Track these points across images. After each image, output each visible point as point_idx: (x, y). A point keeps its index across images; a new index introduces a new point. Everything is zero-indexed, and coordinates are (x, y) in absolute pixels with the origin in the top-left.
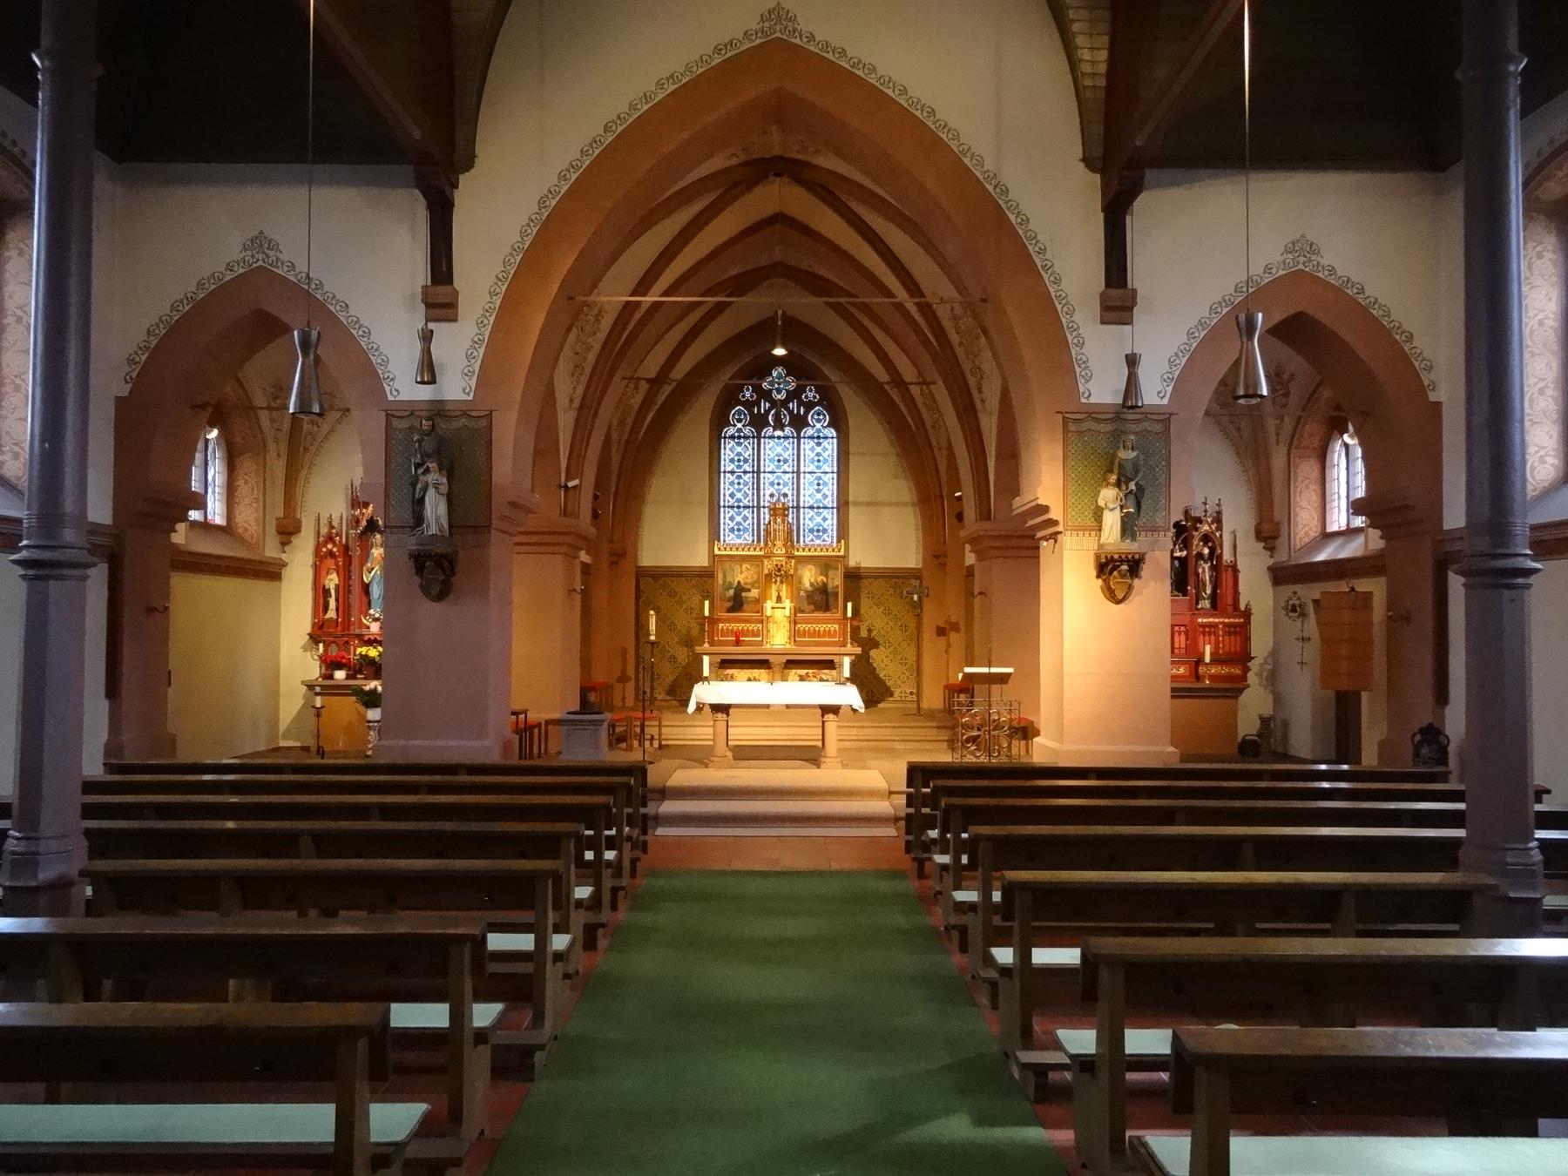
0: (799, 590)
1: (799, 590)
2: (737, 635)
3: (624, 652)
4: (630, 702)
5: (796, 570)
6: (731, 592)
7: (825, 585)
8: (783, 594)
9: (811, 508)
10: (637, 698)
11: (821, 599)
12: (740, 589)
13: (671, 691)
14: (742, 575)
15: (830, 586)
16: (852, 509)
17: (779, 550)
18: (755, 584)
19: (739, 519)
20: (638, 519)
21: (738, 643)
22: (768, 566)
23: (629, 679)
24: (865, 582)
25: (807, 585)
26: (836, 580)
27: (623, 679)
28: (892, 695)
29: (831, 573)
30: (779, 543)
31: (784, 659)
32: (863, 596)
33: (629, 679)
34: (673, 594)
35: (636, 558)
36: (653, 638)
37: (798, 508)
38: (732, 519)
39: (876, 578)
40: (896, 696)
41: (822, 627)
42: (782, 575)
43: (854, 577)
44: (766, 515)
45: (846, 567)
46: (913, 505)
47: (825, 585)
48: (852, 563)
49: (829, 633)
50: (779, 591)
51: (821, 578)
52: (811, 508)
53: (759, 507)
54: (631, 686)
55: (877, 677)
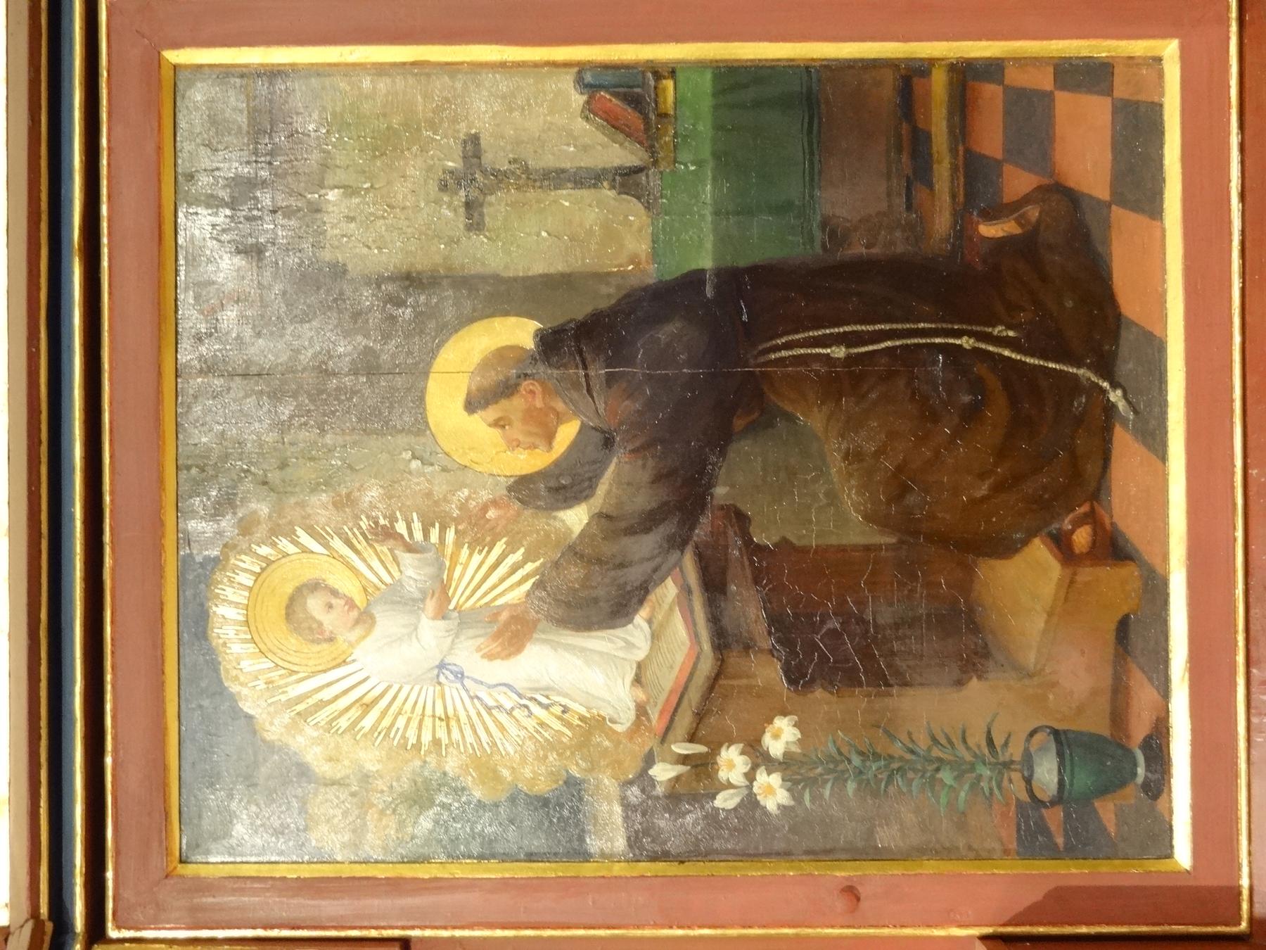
7: (587, 336)
47: (587, 336)
51: (471, 421)
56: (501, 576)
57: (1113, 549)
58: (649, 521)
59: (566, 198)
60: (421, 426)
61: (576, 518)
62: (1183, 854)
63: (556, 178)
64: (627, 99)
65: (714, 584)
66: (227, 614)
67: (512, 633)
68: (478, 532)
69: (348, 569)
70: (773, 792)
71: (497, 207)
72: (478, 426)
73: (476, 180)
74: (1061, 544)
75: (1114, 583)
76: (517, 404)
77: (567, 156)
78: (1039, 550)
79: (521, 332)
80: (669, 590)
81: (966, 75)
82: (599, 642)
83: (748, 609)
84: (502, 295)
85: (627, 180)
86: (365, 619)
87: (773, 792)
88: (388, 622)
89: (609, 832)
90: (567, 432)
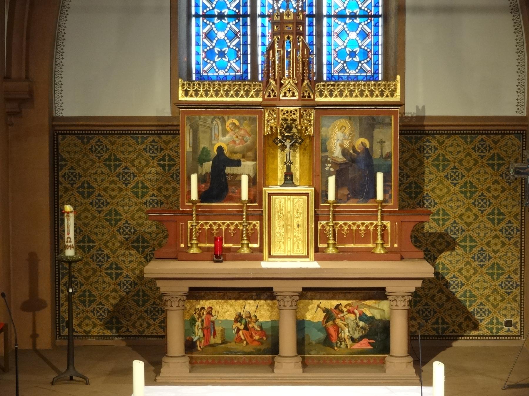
0: (324, 161)
1: (324, 161)
2: (217, 240)
3: (33, 260)
4: (45, 341)
5: (317, 127)
6: (208, 166)
8: (296, 169)
9: (341, 16)
10: (56, 334)
11: (355, 175)
12: (222, 161)
13: (115, 320)
14: (225, 137)
15: (377, 154)
16: (408, 16)
17: (289, 92)
18: (250, 152)
19: (221, 35)
20: (54, 39)
21: (219, 255)
22: (270, 121)
23: (41, 305)
24: (433, 142)
25: (337, 153)
26: (387, 142)
27: (32, 305)
28: (476, 326)
29: (379, 134)
30: (288, 83)
31: (298, 286)
32: (428, 163)
33: (41, 305)
34: (113, 163)
35: (51, 104)
36: (70, 253)
37: (319, 17)
38: (209, 36)
39: (449, 133)
40: (483, 330)
41: (362, 225)
42: (290, 135)
43: (415, 132)
44: (264, 27)
45: (403, 118)
46: (513, 10)
47: (368, 153)
48: (410, 110)
49: (369, 236)
50: (288, 164)
51: (360, 142)
52: (341, 16)
53: (254, 16)
54: (45, 317)
55: (451, 297)
56: (346, 144)
57: (348, 199)
58: (351, 158)
59: (380, 150)
60: (360, 137)
61: (351, 151)
62: (321, 204)
63: (382, 150)
64: (389, 156)
65: (345, 164)
66: (342, 120)
67: (341, 146)
68: (350, 143)
69: (347, 132)
70: (327, 169)
71: (379, 144)
72: (360, 143)
73: (382, 142)
74: (349, 194)
75: (345, 198)
76: (362, 146)
77: (383, 151)
78: (348, 192)
79: (368, 146)
80: (345, 160)
81: (391, 186)
82: (340, 153)
83: (343, 167)
84: (371, 144)
85: (382, 156)
86: (343, 133)
87: (327, 169)
88: (342, 135)
89: (324, 154)
90: (359, 151)
